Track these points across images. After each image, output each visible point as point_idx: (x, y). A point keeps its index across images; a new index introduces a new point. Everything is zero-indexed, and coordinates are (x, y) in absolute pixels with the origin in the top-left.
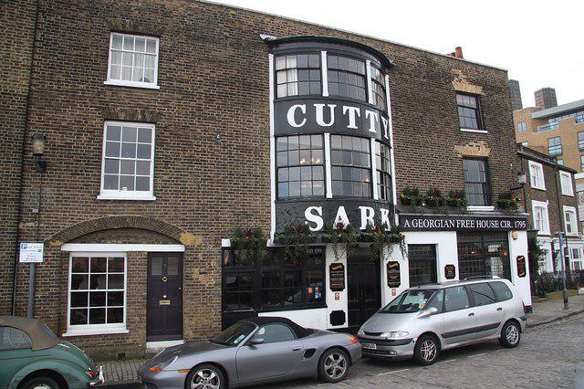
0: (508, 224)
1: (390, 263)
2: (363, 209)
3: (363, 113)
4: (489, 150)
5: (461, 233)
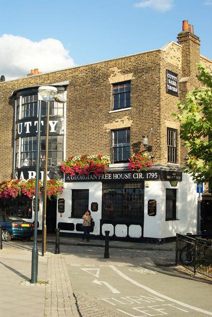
0: (140, 176)
1: (60, 199)
2: (30, 173)
3: (33, 123)
4: (131, 121)
5: (104, 182)
